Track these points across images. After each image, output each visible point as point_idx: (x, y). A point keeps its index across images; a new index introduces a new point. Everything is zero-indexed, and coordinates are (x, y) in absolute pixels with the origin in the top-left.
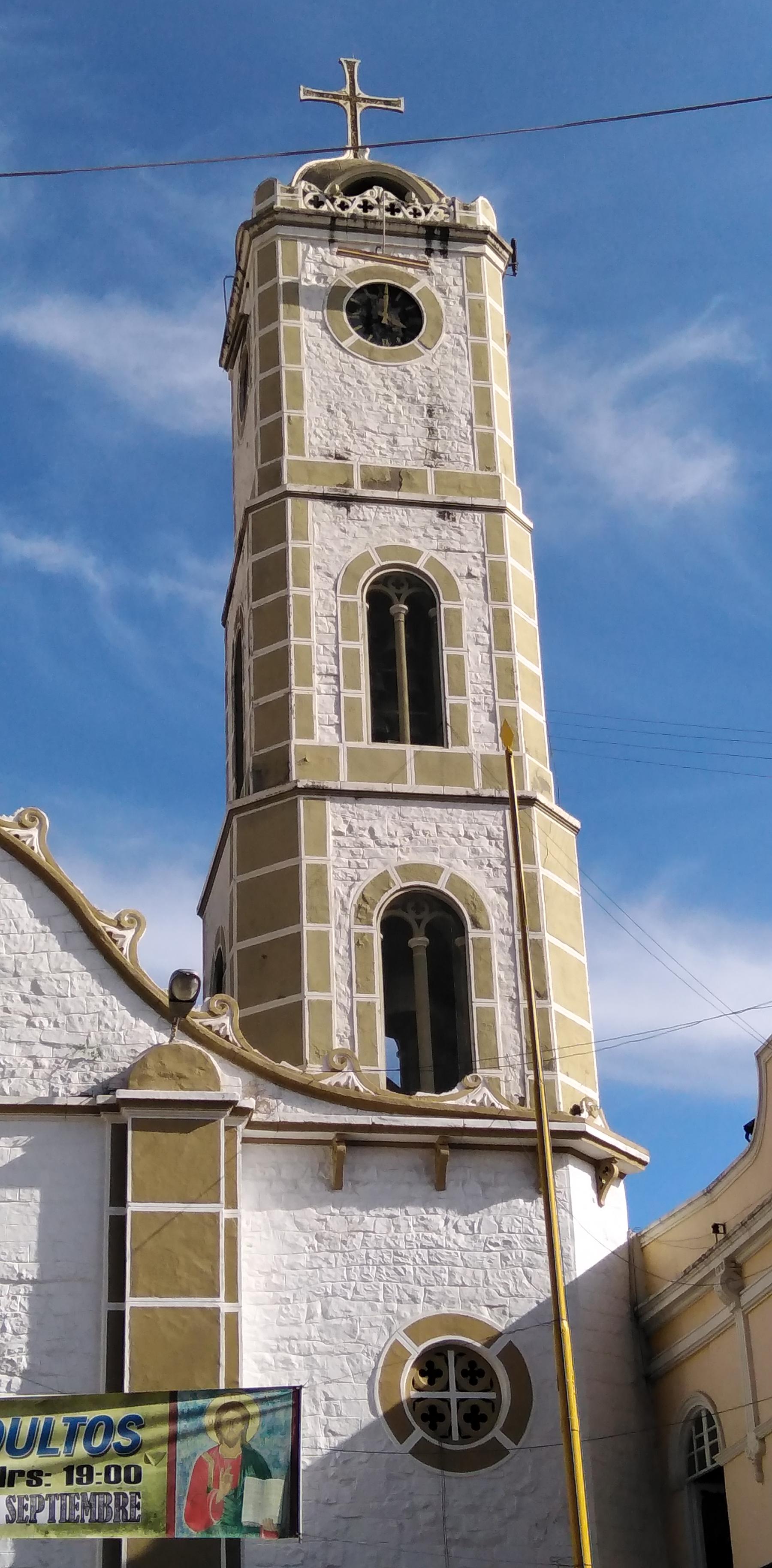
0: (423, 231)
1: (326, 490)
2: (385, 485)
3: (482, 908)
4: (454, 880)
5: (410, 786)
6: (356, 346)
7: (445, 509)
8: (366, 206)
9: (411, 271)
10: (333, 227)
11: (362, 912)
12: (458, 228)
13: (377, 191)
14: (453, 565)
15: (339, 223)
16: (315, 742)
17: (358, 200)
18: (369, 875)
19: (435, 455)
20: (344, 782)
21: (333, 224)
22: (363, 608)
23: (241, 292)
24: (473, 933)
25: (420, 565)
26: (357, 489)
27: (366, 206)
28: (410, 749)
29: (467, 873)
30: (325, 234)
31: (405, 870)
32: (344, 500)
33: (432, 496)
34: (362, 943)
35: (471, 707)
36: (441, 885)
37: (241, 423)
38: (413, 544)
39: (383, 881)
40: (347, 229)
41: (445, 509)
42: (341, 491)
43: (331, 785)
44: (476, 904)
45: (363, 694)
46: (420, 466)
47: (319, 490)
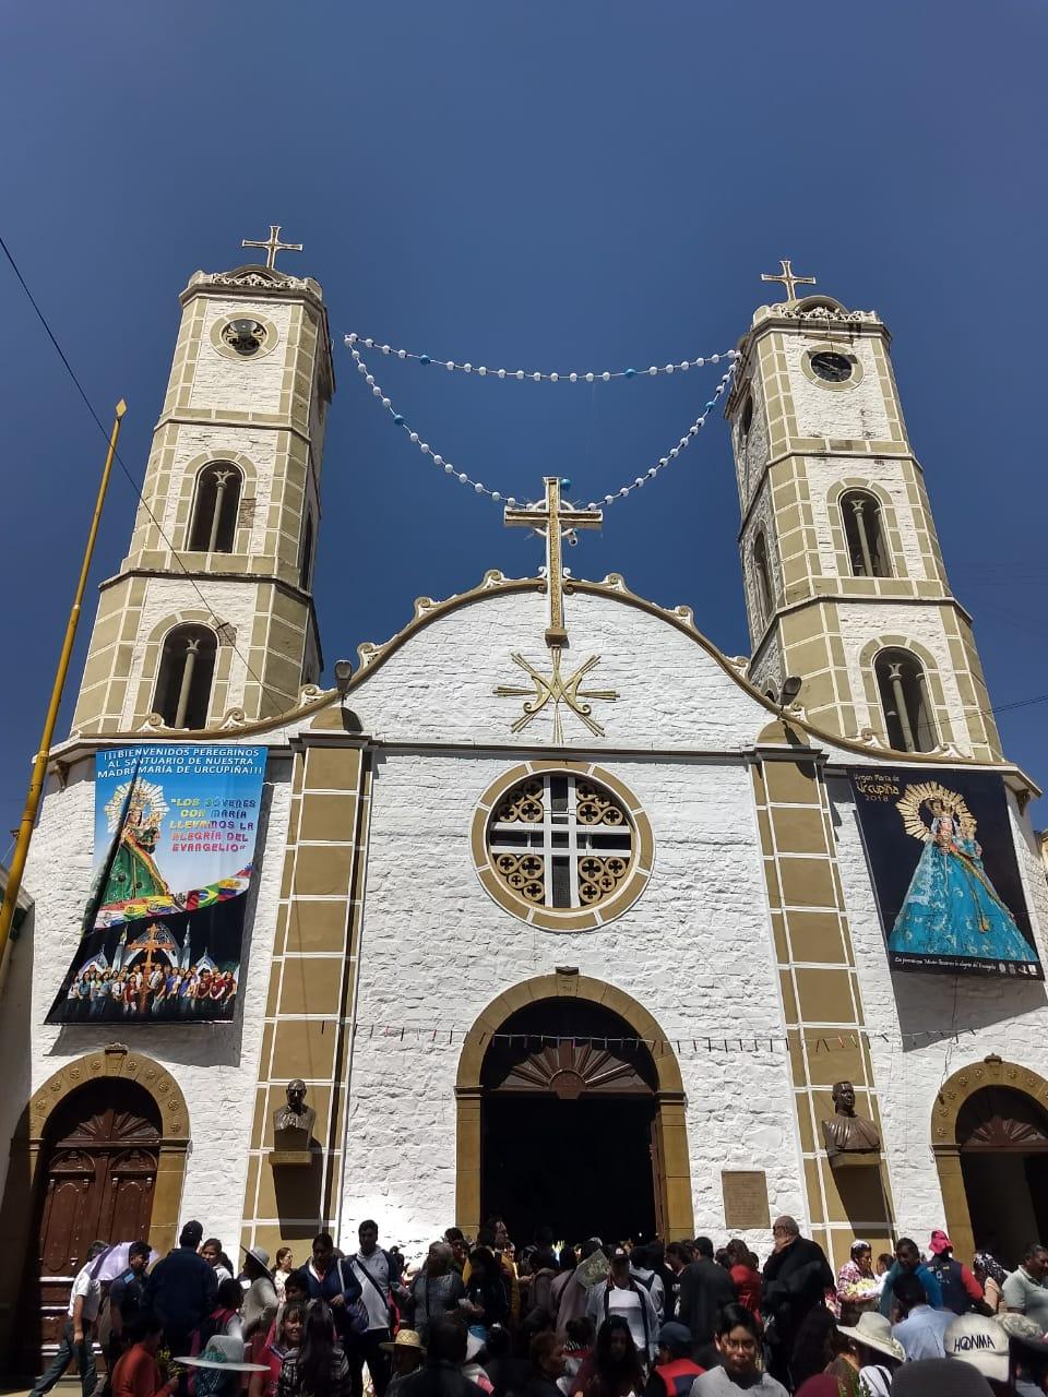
0: (847, 326)
1: (813, 451)
2: (843, 449)
3: (932, 658)
4: (914, 643)
5: (878, 596)
6: (818, 383)
7: (879, 458)
8: (814, 316)
9: (841, 345)
10: (799, 327)
11: (864, 661)
12: (866, 324)
13: (820, 310)
14: (888, 487)
15: (803, 324)
16: (822, 577)
17: (810, 313)
18: (865, 642)
19: (869, 434)
20: (840, 594)
21: (800, 325)
22: (839, 510)
23: (744, 369)
24: (927, 671)
25: (869, 487)
26: (828, 451)
27: (814, 316)
28: (876, 579)
29: (920, 640)
30: (797, 331)
31: (883, 638)
32: (823, 456)
33: (869, 452)
34: (866, 676)
35: (906, 558)
36: (907, 646)
37: (745, 437)
38: (866, 477)
39: (873, 642)
40: (807, 327)
41: (879, 458)
42: (821, 451)
43: (837, 595)
44: (928, 656)
45: (846, 553)
46: (860, 439)
47: (810, 452)
